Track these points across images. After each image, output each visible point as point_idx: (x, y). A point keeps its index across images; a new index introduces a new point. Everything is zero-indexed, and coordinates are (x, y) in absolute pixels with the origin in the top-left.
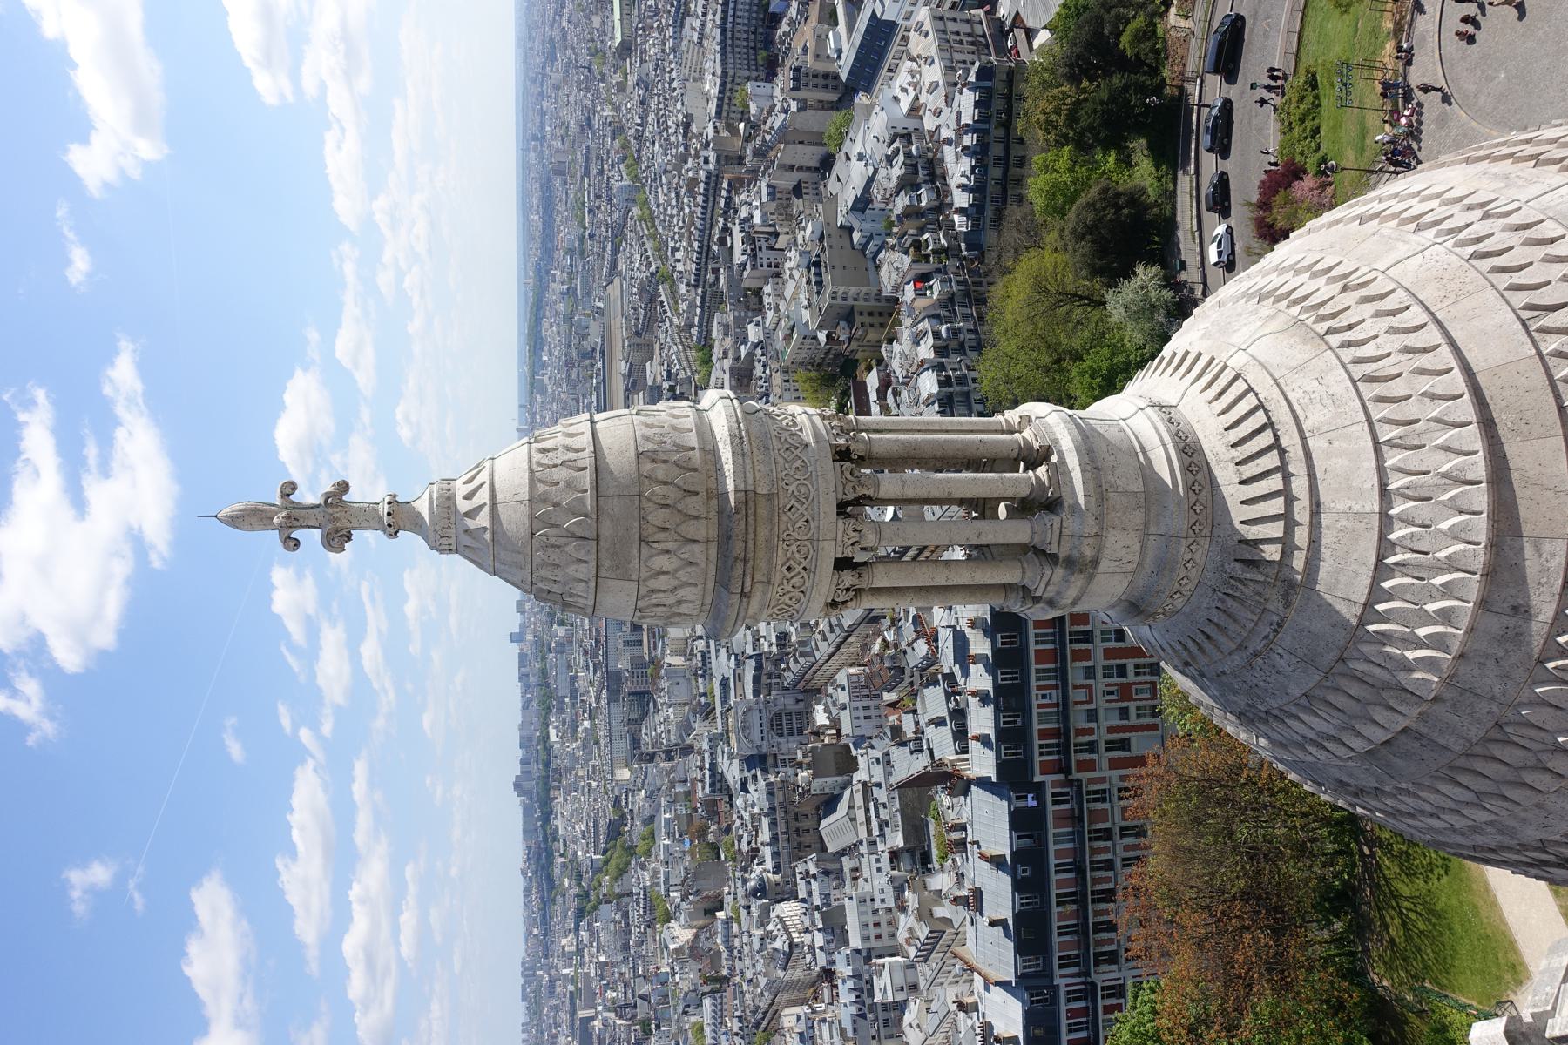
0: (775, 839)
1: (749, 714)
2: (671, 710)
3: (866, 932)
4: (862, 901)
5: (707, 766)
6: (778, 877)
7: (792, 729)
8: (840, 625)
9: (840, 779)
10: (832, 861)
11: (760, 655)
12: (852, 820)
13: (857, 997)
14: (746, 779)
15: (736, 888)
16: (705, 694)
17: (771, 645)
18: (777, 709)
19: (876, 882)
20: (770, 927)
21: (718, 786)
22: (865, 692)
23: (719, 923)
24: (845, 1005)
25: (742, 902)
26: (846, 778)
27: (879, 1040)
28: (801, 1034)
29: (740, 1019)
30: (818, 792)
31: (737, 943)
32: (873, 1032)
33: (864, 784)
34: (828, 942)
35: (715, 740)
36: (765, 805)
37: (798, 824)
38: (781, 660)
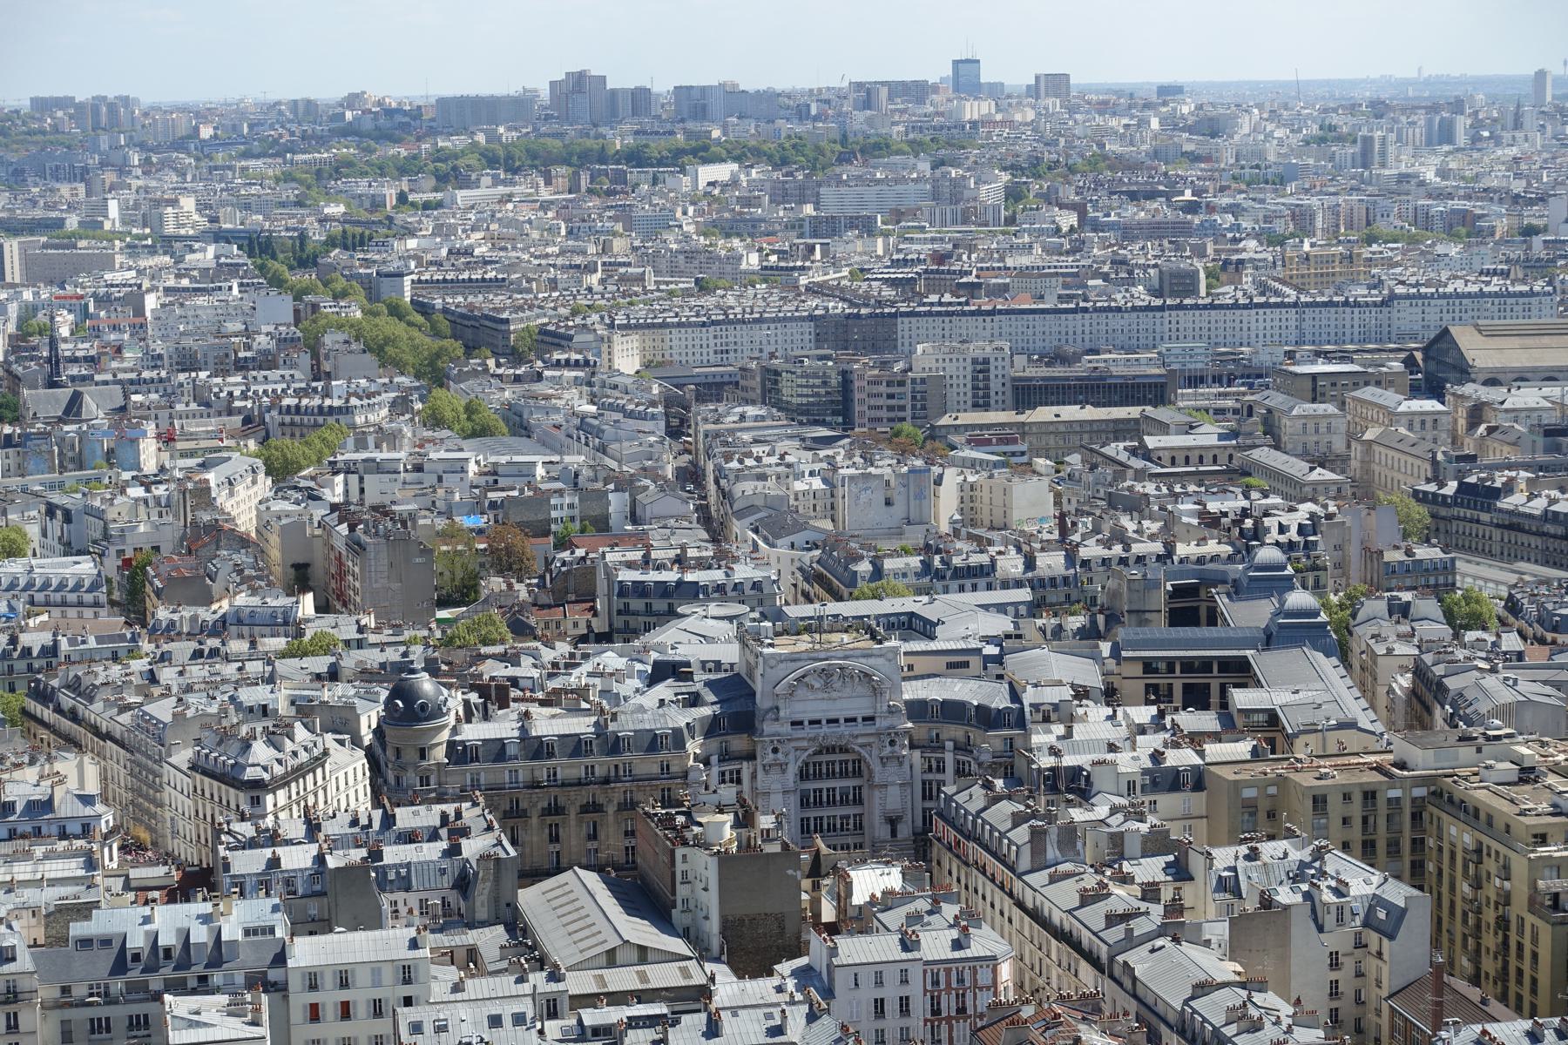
0: (537, 749)
1: (861, 689)
2: (817, 484)
3: (329, 980)
4: (407, 974)
5: (690, 577)
6: (439, 754)
7: (818, 803)
8: (1130, 942)
9: (713, 926)
10: (495, 899)
11: (1021, 722)
12: (611, 953)
13: (168, 951)
14: (688, 677)
15: (382, 646)
16: (878, 573)
17: (1054, 752)
18: (876, 767)
19: (463, 1011)
20: (301, 733)
21: (637, 604)
22: (948, 1004)
23: (284, 601)
24: (147, 920)
25: (350, 660)
26: (715, 942)
27: (59, 1006)
28: (48, 805)
29: (51, 651)
30: (680, 867)
31: (238, 646)
32: (79, 991)
33: (703, 993)
34: (288, 882)
35: (756, 593)
36: (625, 725)
37: (611, 809)
38: (1010, 775)
